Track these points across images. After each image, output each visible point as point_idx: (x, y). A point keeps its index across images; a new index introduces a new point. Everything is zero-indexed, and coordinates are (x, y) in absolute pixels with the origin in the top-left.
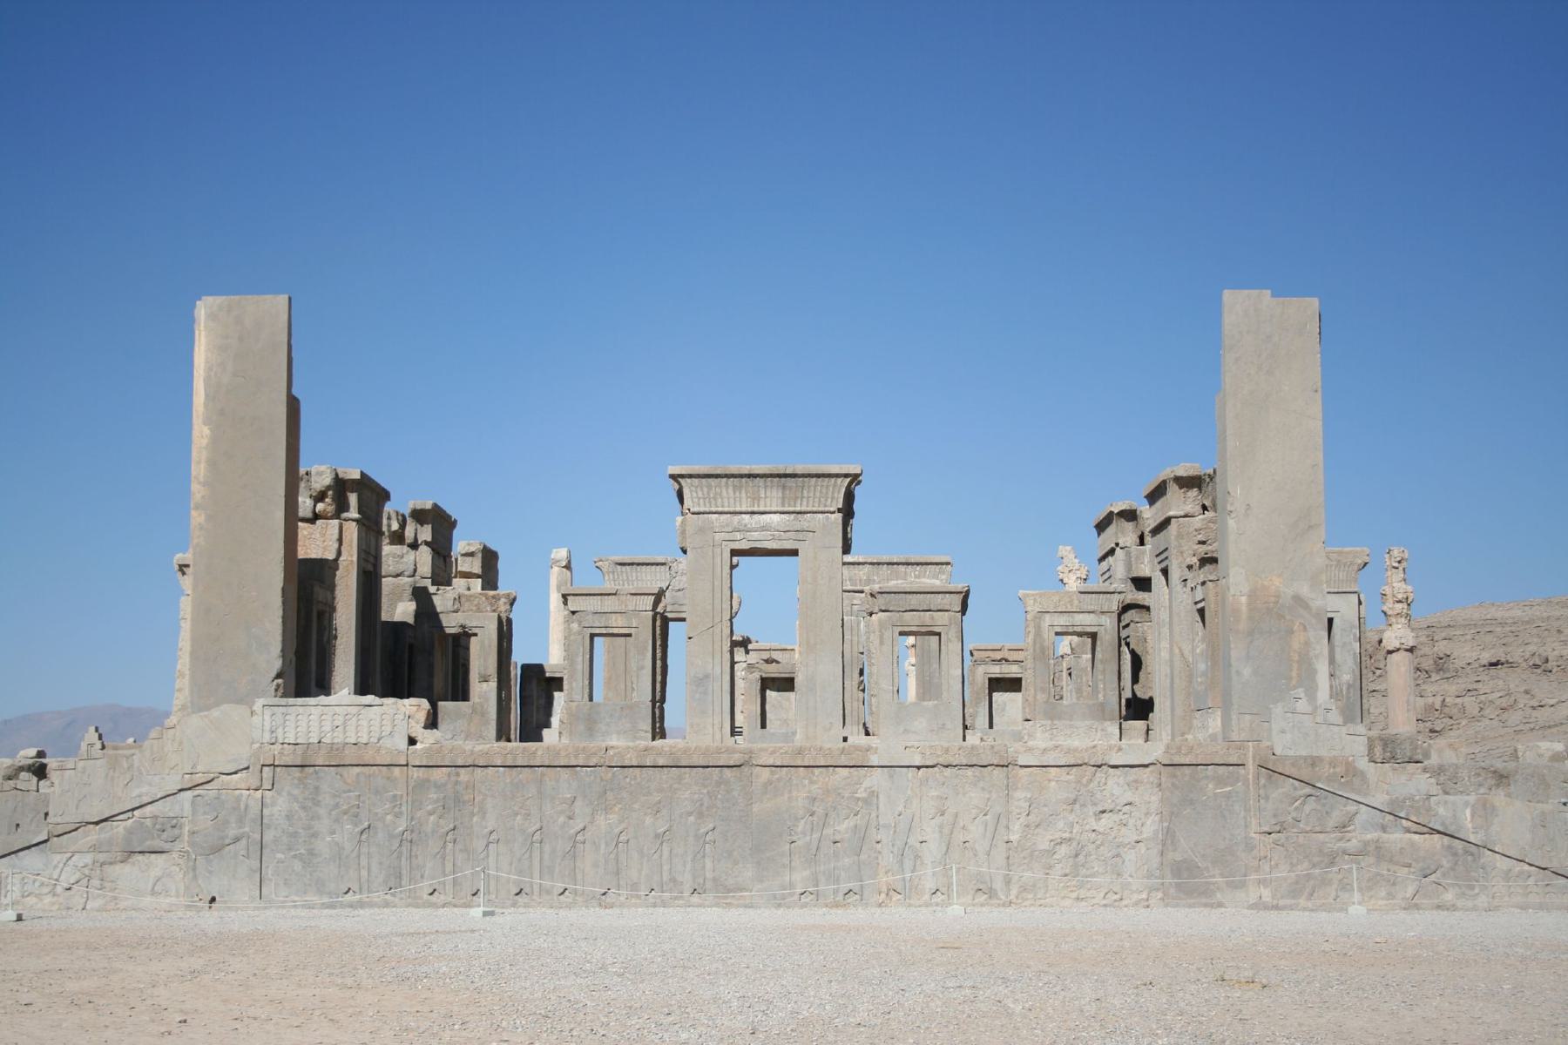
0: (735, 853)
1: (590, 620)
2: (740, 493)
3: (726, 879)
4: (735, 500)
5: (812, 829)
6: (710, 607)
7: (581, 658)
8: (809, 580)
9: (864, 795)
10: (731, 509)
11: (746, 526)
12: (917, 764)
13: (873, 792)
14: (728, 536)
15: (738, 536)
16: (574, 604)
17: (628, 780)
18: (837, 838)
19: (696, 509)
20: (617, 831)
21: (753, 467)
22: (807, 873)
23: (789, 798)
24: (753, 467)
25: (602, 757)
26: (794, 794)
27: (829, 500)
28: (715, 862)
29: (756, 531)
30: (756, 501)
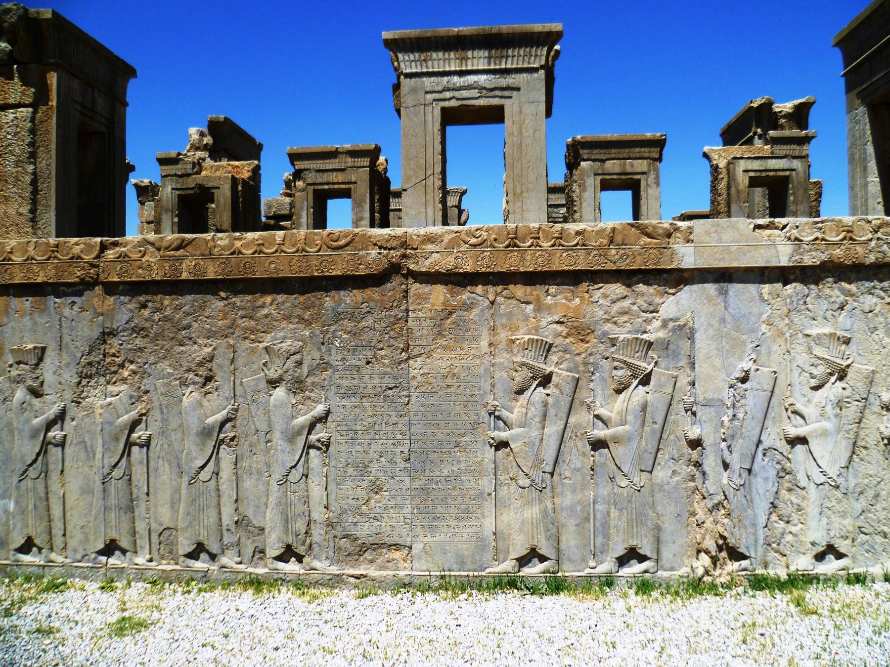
0: (374, 468)
1: (311, 177)
2: (449, 55)
3: (355, 524)
4: (444, 63)
5: (545, 416)
6: (422, 161)
7: (305, 212)
8: (515, 133)
9: (661, 334)
10: (441, 70)
11: (454, 84)
12: (784, 262)
13: (681, 328)
14: (437, 96)
15: (448, 95)
16: (300, 165)
17: (146, 313)
18: (600, 432)
19: (408, 71)
20: (126, 418)
21: (461, 28)
22: (533, 512)
23: (490, 345)
24: (461, 28)
25: (93, 265)
26: (503, 335)
27: (533, 58)
28: (332, 487)
29: (465, 90)
30: (464, 62)
